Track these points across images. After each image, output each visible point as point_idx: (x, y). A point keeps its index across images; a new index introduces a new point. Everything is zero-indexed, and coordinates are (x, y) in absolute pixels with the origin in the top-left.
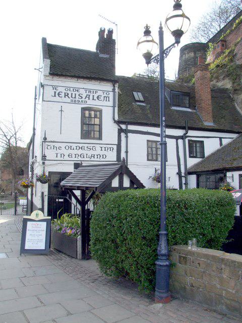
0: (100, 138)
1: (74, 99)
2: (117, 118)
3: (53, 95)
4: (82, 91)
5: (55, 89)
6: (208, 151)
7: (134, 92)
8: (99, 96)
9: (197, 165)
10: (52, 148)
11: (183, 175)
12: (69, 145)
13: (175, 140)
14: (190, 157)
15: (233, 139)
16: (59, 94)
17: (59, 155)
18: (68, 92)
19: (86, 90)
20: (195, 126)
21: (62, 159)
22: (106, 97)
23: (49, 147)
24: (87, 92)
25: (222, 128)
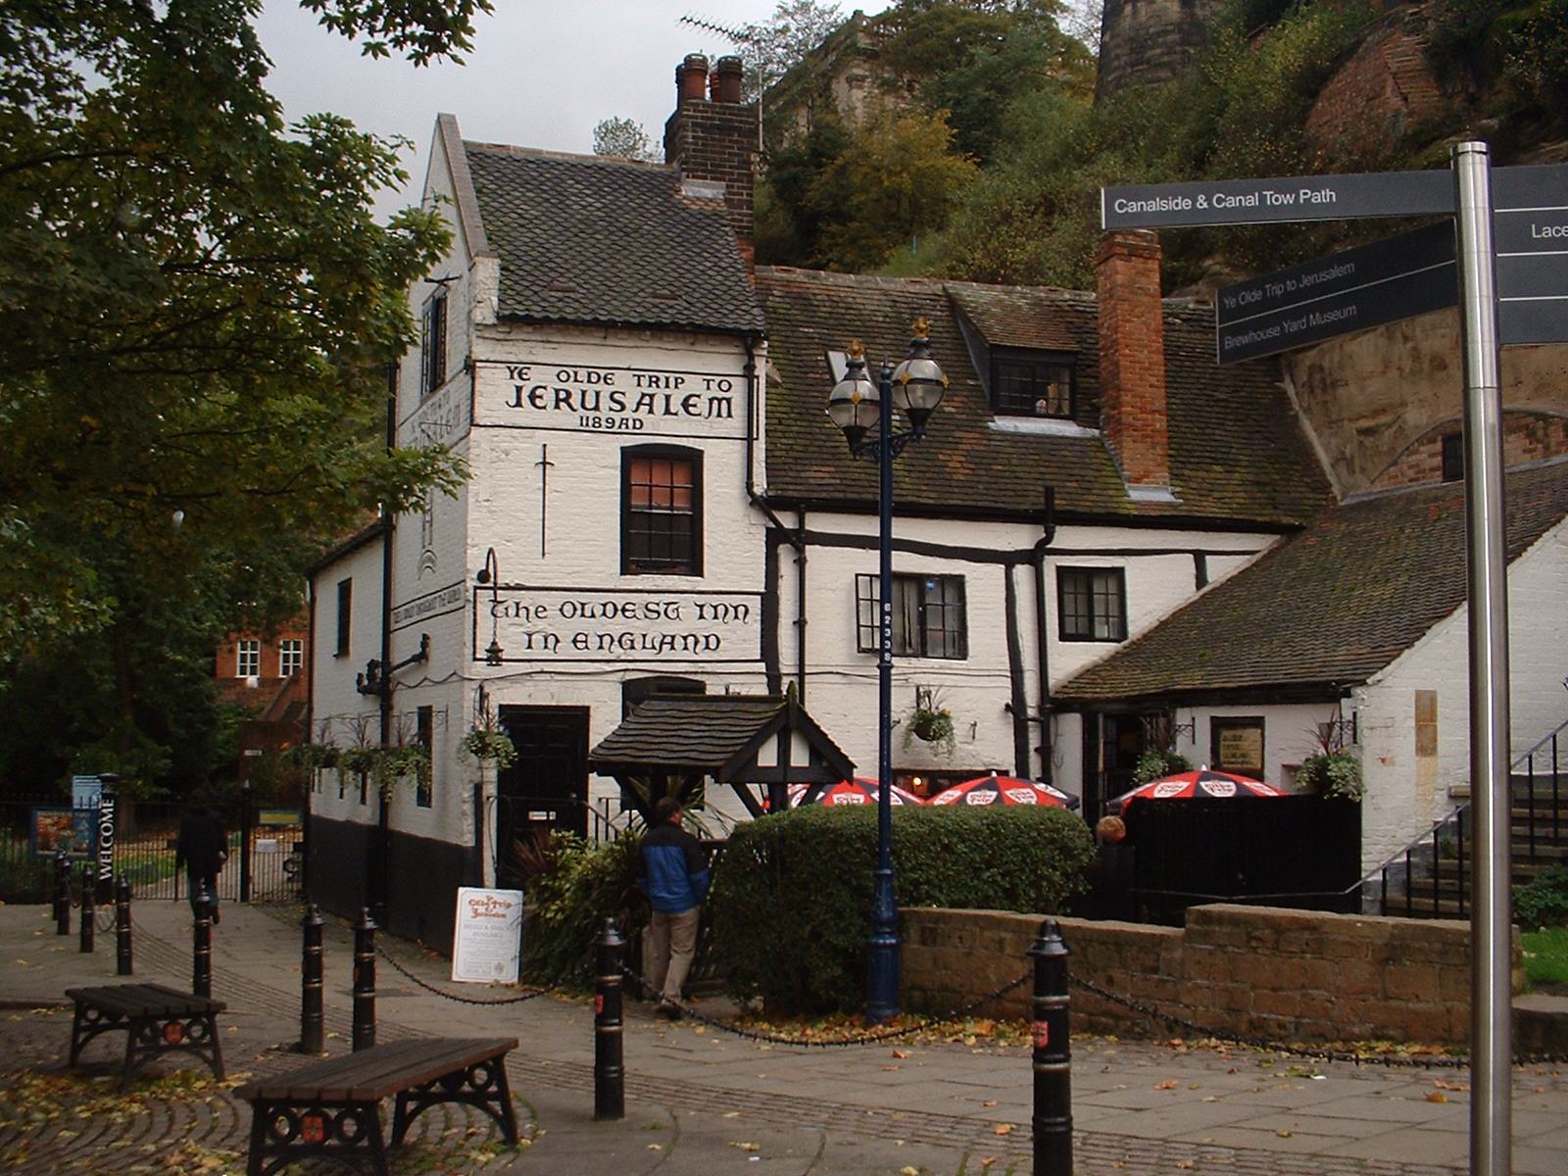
0: (696, 569)
1: (592, 414)
2: (760, 486)
3: (513, 402)
4: (623, 382)
5: (520, 374)
6: (1142, 616)
7: (832, 354)
8: (687, 399)
9: (1091, 673)
10: (512, 611)
11: (1031, 712)
12: (576, 597)
16: (533, 397)
17: (537, 638)
18: (570, 386)
19: (638, 374)
20: (1083, 506)
21: (549, 654)
22: (720, 401)
23: (500, 608)
24: (645, 382)
25: (1211, 509)
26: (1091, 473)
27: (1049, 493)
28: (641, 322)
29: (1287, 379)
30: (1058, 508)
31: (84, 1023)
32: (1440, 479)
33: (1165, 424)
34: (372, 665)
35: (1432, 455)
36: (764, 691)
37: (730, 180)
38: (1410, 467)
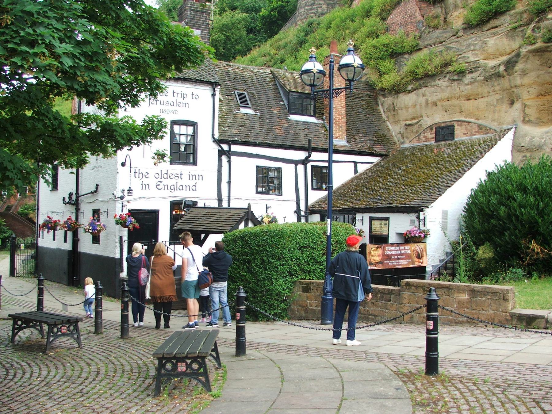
0: (195, 163)
2: (217, 136)
9: (321, 201)
11: (303, 213)
13: (294, 165)
14: (313, 189)
15: (372, 165)
26: (321, 135)
27: (310, 141)
28: (178, 78)
29: (380, 106)
30: (312, 146)
31: (16, 326)
32: (434, 141)
33: (345, 119)
34: (71, 195)
35: (431, 134)
36: (216, 205)
37: (202, 30)
38: (424, 137)
